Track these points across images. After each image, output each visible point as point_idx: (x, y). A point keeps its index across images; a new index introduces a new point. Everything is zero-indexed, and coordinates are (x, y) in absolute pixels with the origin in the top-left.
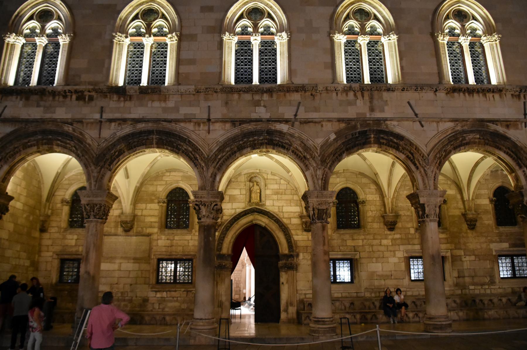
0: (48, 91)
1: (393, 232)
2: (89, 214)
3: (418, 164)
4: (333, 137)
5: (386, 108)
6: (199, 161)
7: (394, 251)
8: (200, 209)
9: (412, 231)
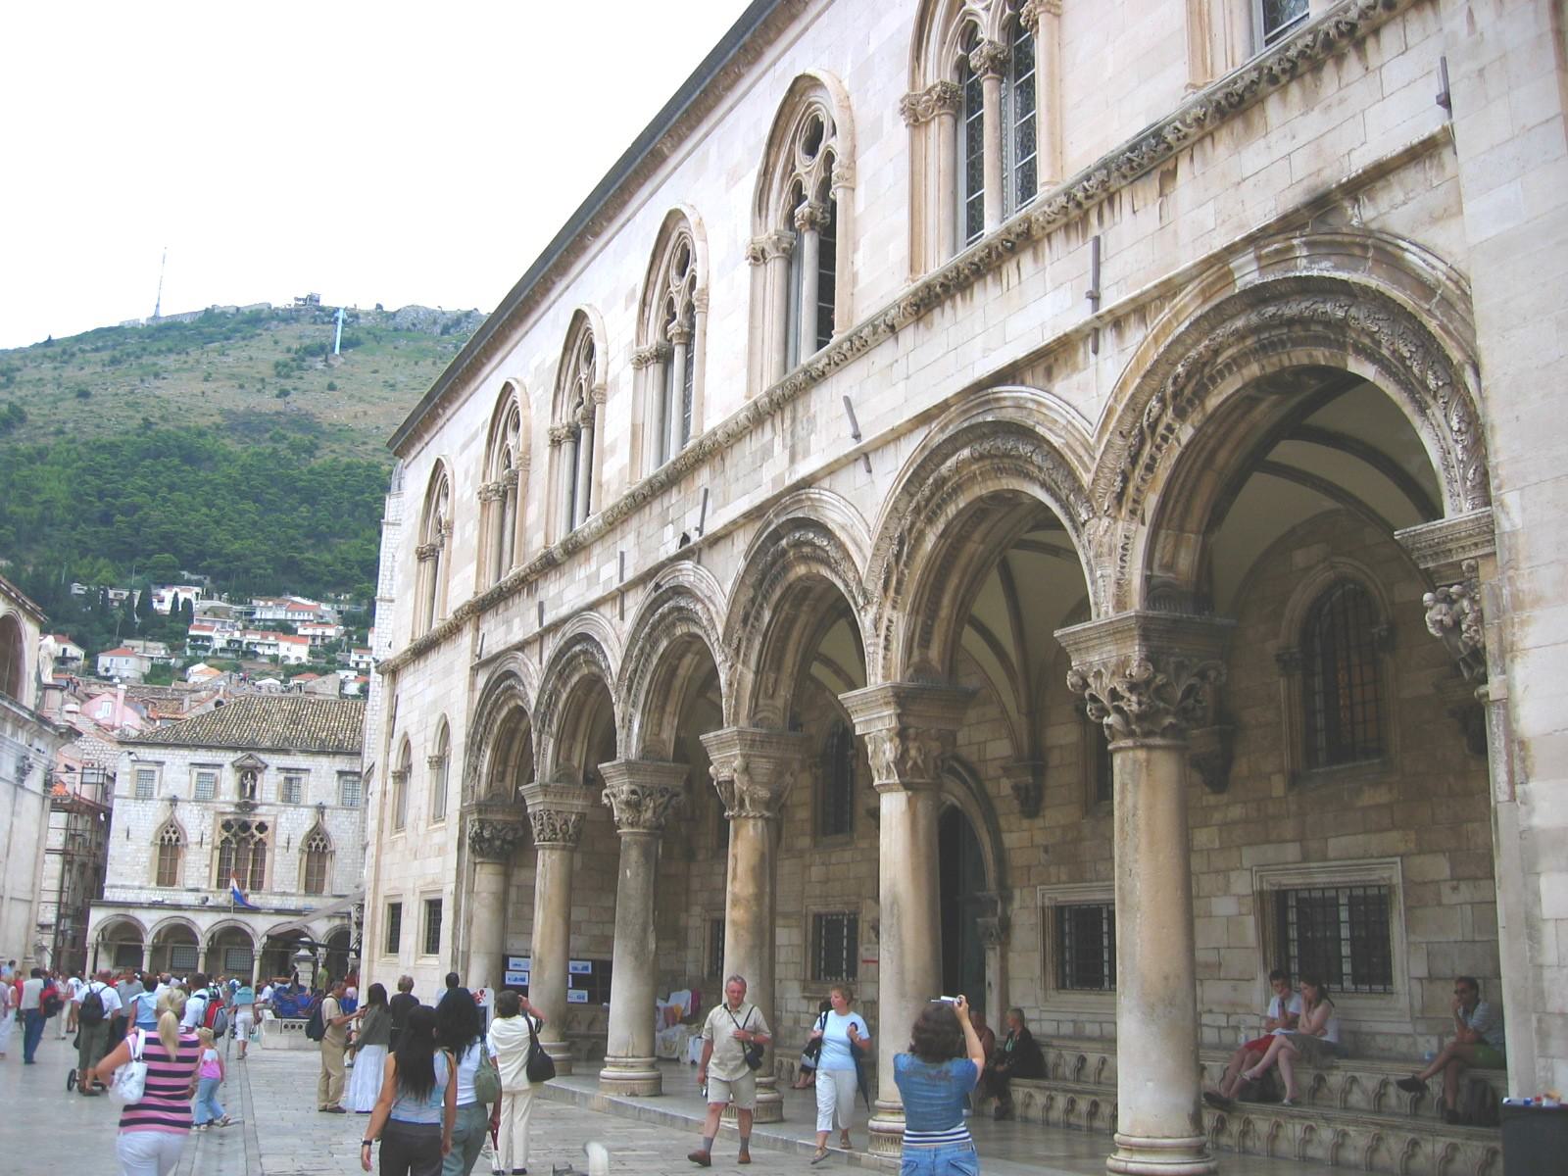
1: (1225, 798)
7: (1225, 872)
9: (1278, 786)
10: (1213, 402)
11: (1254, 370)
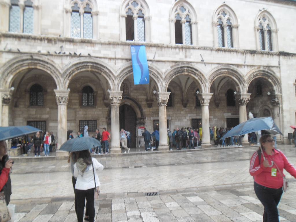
0: (32, 38)
1: (185, 108)
2: (60, 101)
3: (203, 82)
4: (169, 68)
5: (192, 56)
6: (112, 77)
7: (186, 116)
8: (113, 99)
9: (193, 108)
10: (256, 77)
11: (260, 76)
